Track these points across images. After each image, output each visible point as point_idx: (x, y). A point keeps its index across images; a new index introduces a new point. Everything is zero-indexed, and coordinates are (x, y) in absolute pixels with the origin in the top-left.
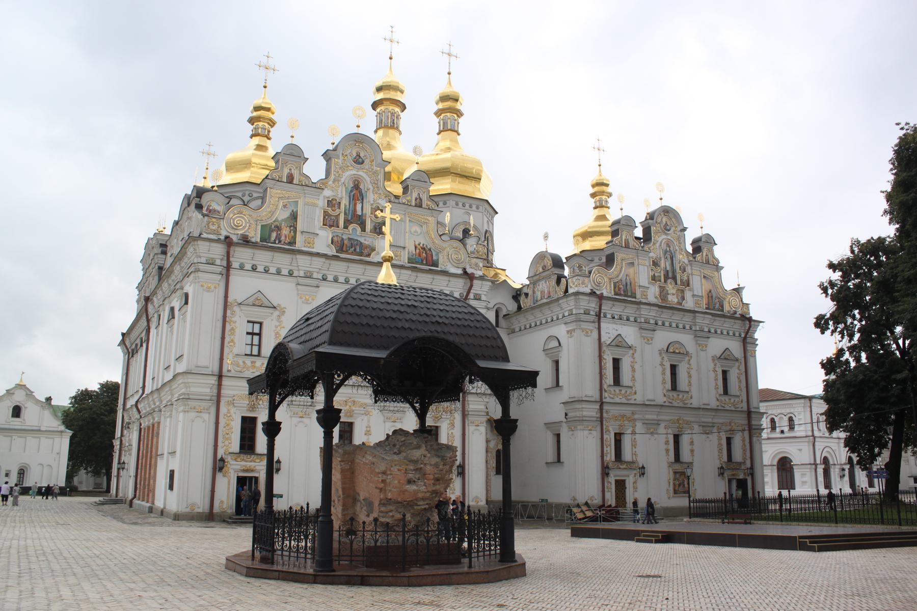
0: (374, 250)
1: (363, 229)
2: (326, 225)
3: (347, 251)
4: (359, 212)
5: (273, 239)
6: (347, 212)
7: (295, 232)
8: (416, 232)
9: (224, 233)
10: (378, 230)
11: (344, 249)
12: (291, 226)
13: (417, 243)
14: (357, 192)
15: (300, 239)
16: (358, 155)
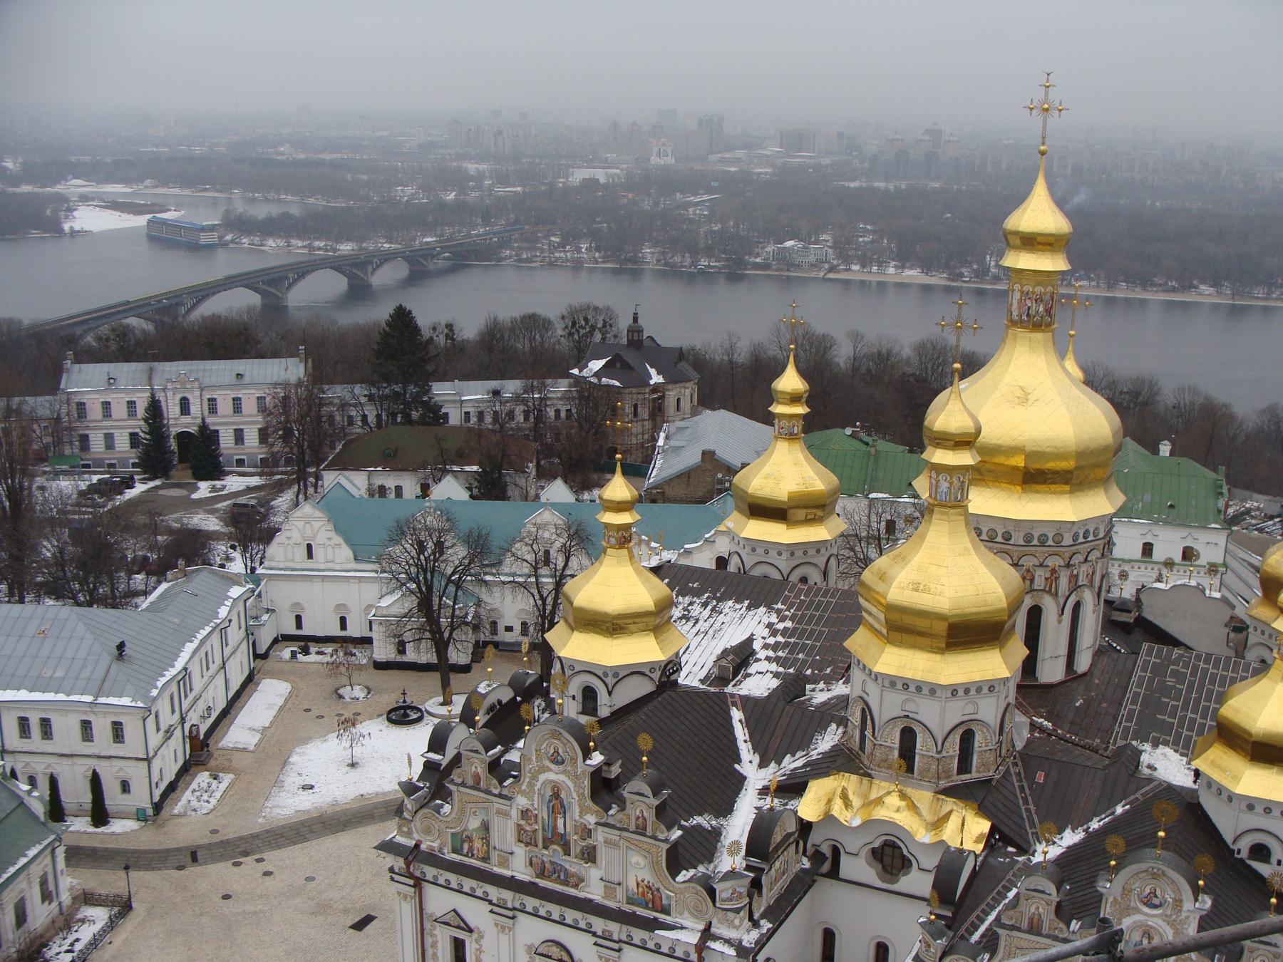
0: (583, 881)
1: (567, 853)
2: (522, 842)
3: (549, 877)
4: (561, 830)
5: (465, 851)
6: (546, 827)
7: (488, 846)
8: (638, 864)
9: (416, 836)
10: (586, 855)
11: (546, 874)
12: (483, 839)
13: (639, 879)
14: (556, 802)
15: (494, 856)
16: (556, 752)
